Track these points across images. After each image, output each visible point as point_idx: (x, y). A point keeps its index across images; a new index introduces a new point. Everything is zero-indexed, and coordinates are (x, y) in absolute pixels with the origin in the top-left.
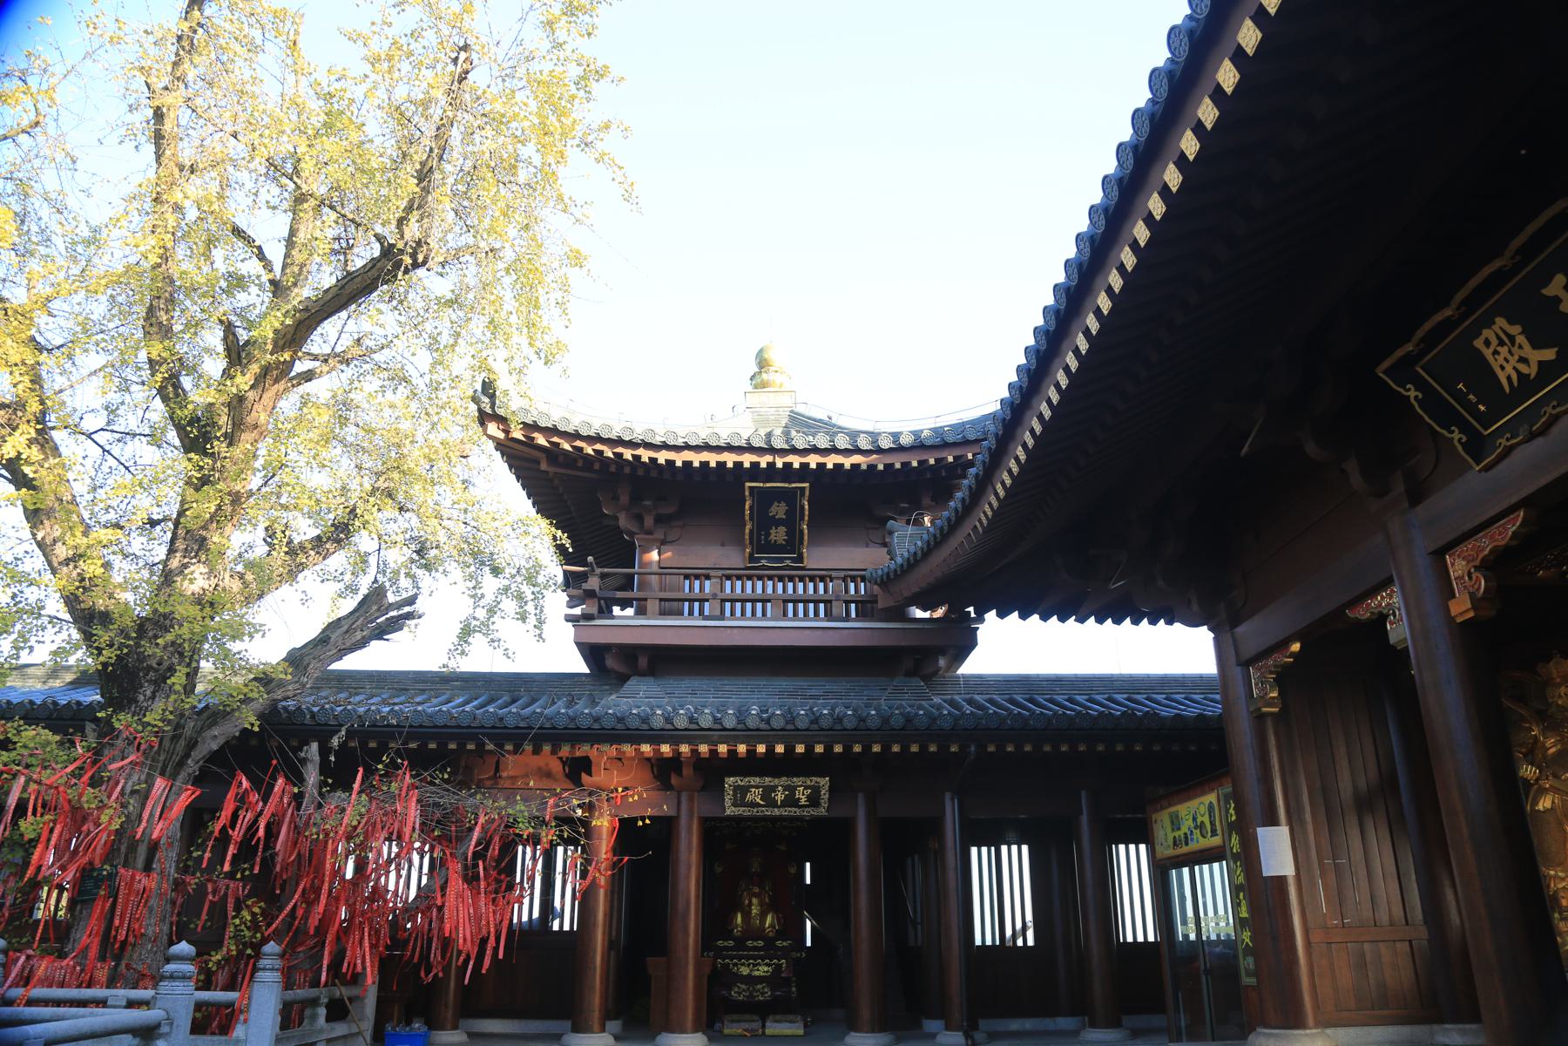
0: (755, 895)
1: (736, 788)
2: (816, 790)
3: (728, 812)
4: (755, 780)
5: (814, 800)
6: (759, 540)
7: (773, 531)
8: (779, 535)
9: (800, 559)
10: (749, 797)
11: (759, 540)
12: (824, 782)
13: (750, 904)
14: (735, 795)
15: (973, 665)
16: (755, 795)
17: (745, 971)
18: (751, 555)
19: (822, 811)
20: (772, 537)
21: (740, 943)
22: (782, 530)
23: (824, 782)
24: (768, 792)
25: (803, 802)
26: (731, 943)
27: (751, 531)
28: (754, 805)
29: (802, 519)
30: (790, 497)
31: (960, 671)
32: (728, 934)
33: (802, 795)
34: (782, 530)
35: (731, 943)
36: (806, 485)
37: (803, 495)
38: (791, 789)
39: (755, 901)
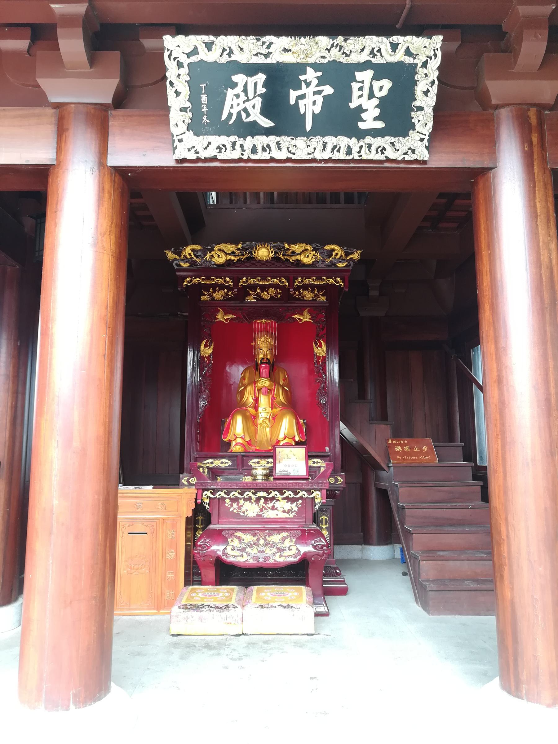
0: (269, 391)
1: (199, 72)
2: (402, 76)
3: (182, 152)
4: (245, 48)
5: (396, 116)
12: (426, 51)
13: (256, 406)
14: (194, 98)
16: (244, 99)
17: (251, 509)
19: (414, 147)
21: (241, 462)
23: (426, 51)
24: (280, 80)
25: (370, 120)
26: (225, 463)
32: (220, 447)
33: (367, 97)
35: (225, 463)
38: (339, 75)
39: (264, 400)
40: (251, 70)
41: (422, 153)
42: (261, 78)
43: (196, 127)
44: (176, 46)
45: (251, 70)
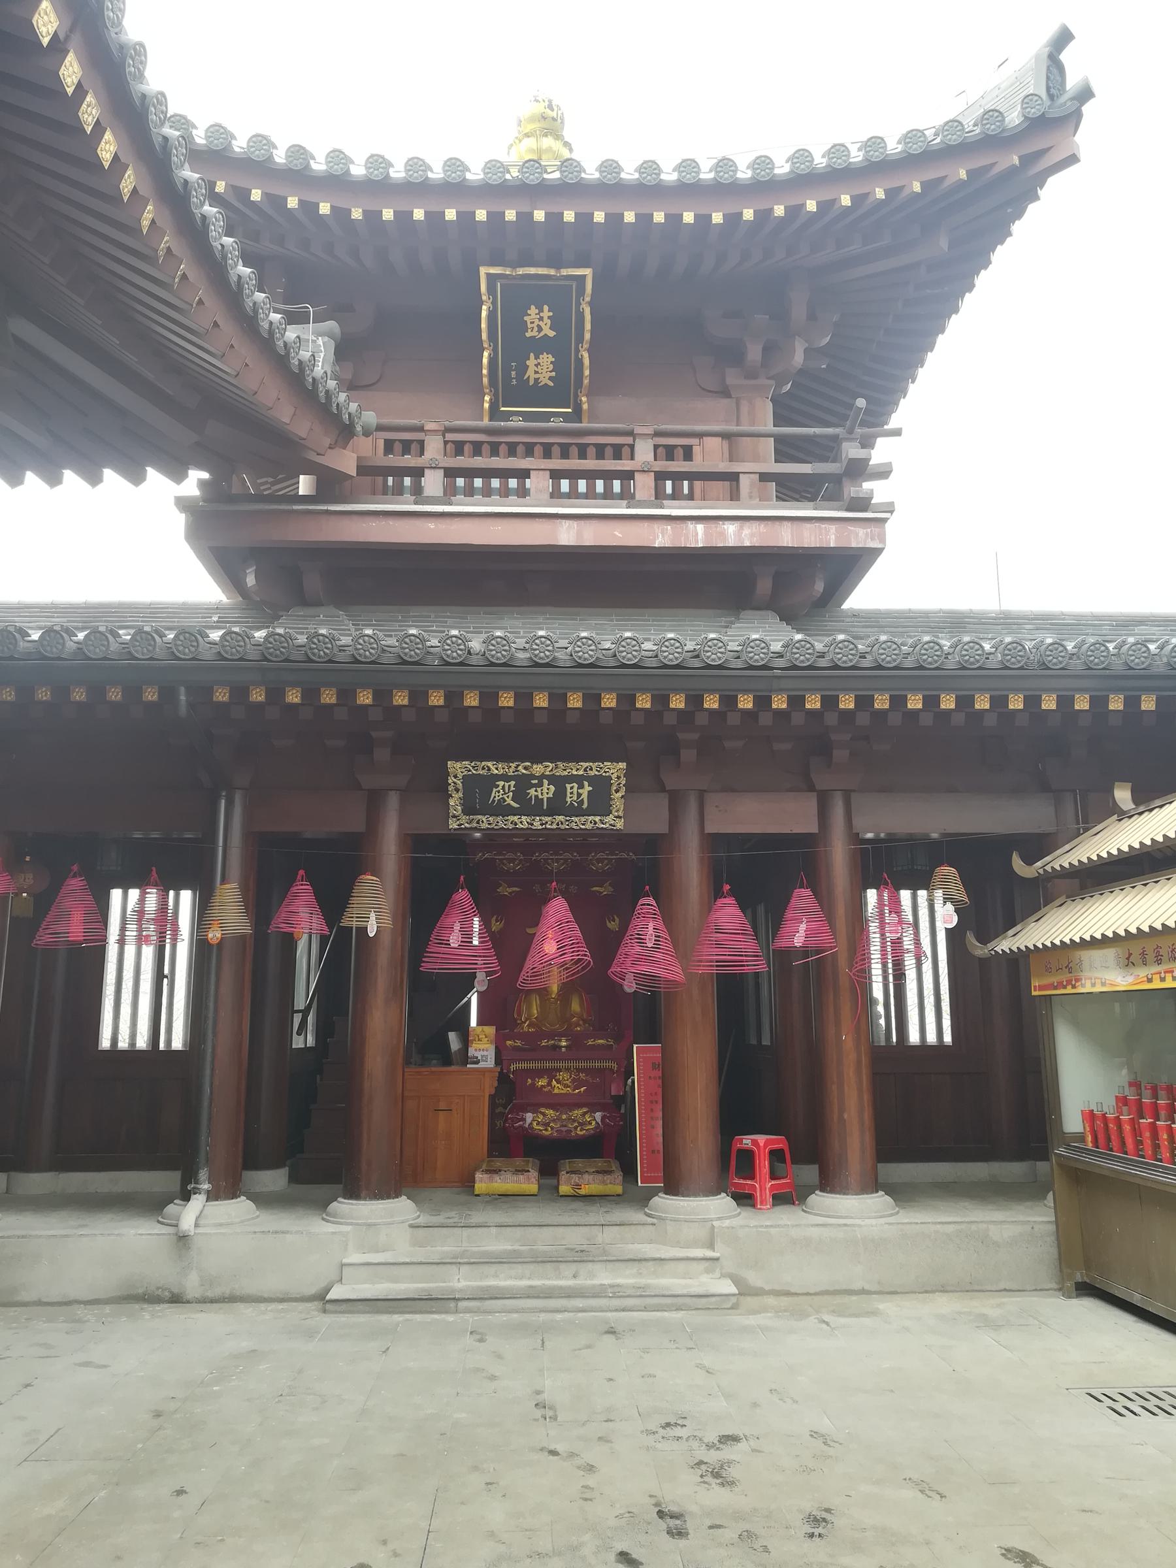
6: (507, 378)
7: (531, 362)
8: (541, 368)
9: (577, 415)
10: (496, 795)
11: (507, 378)
15: (865, 596)
18: (494, 406)
19: (614, 821)
20: (530, 373)
22: (547, 359)
23: (615, 770)
27: (493, 361)
28: (502, 810)
29: (580, 339)
30: (560, 298)
31: (848, 605)
34: (547, 359)
36: (587, 272)
37: (581, 291)
40: (506, 778)
41: (620, 824)
42: (513, 783)
43: (469, 810)
44: (458, 769)
45: (506, 778)
